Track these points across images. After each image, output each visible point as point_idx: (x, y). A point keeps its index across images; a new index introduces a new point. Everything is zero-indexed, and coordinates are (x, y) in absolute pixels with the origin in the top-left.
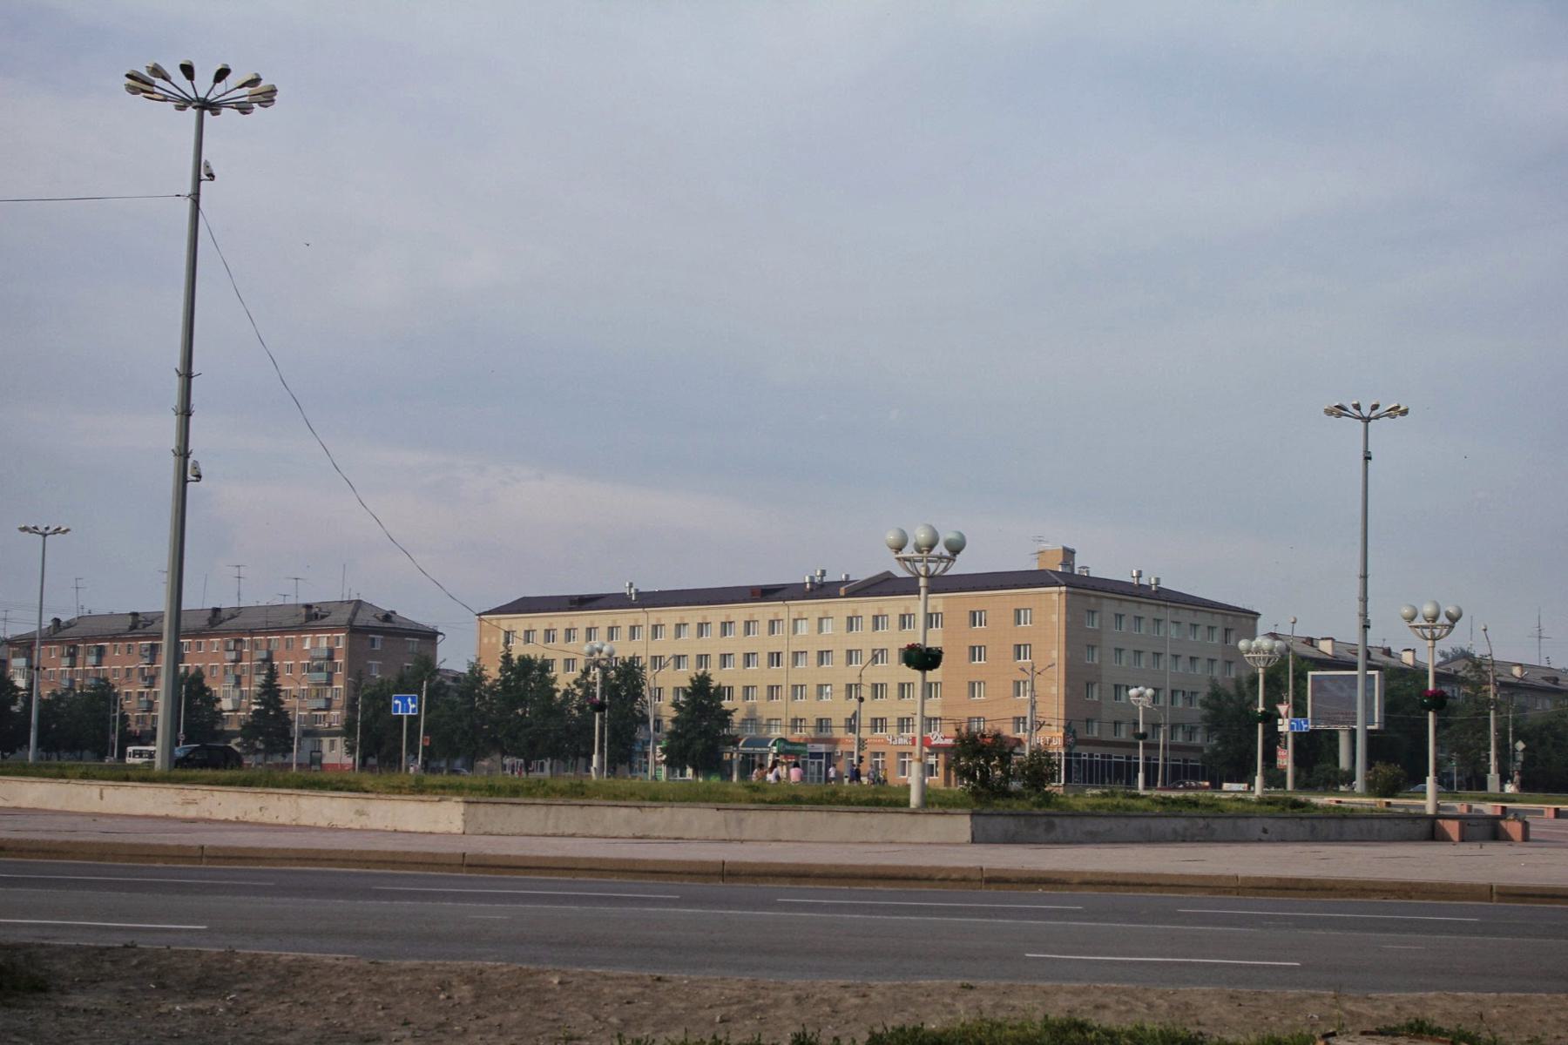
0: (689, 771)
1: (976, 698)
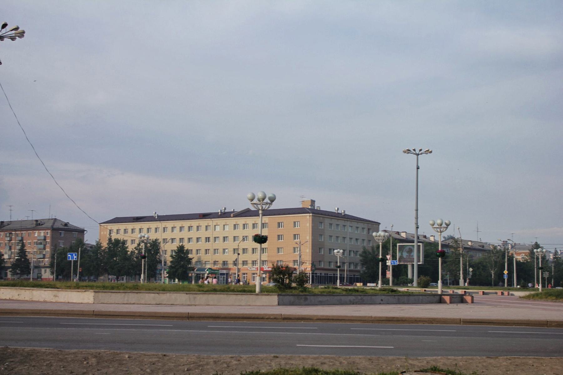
0: (177, 280)
1: (280, 253)
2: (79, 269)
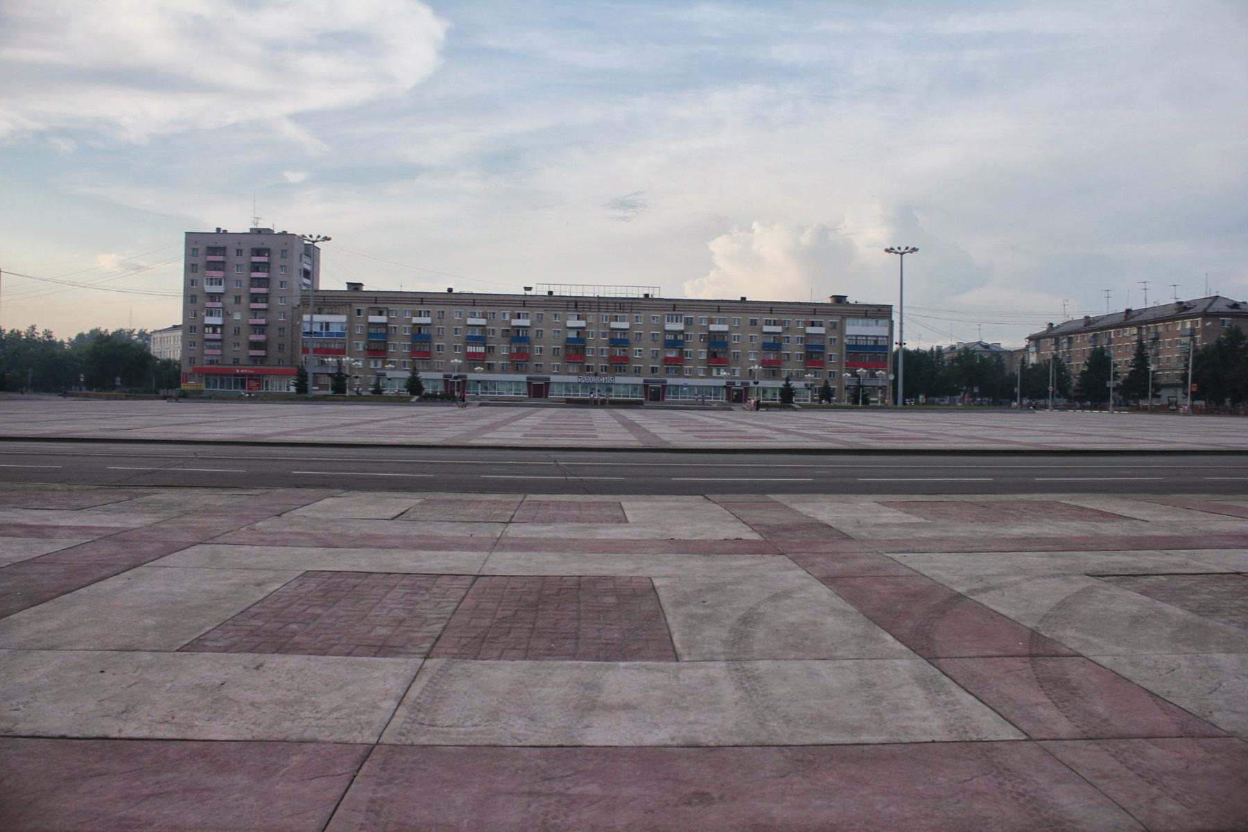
2: (1191, 388)
